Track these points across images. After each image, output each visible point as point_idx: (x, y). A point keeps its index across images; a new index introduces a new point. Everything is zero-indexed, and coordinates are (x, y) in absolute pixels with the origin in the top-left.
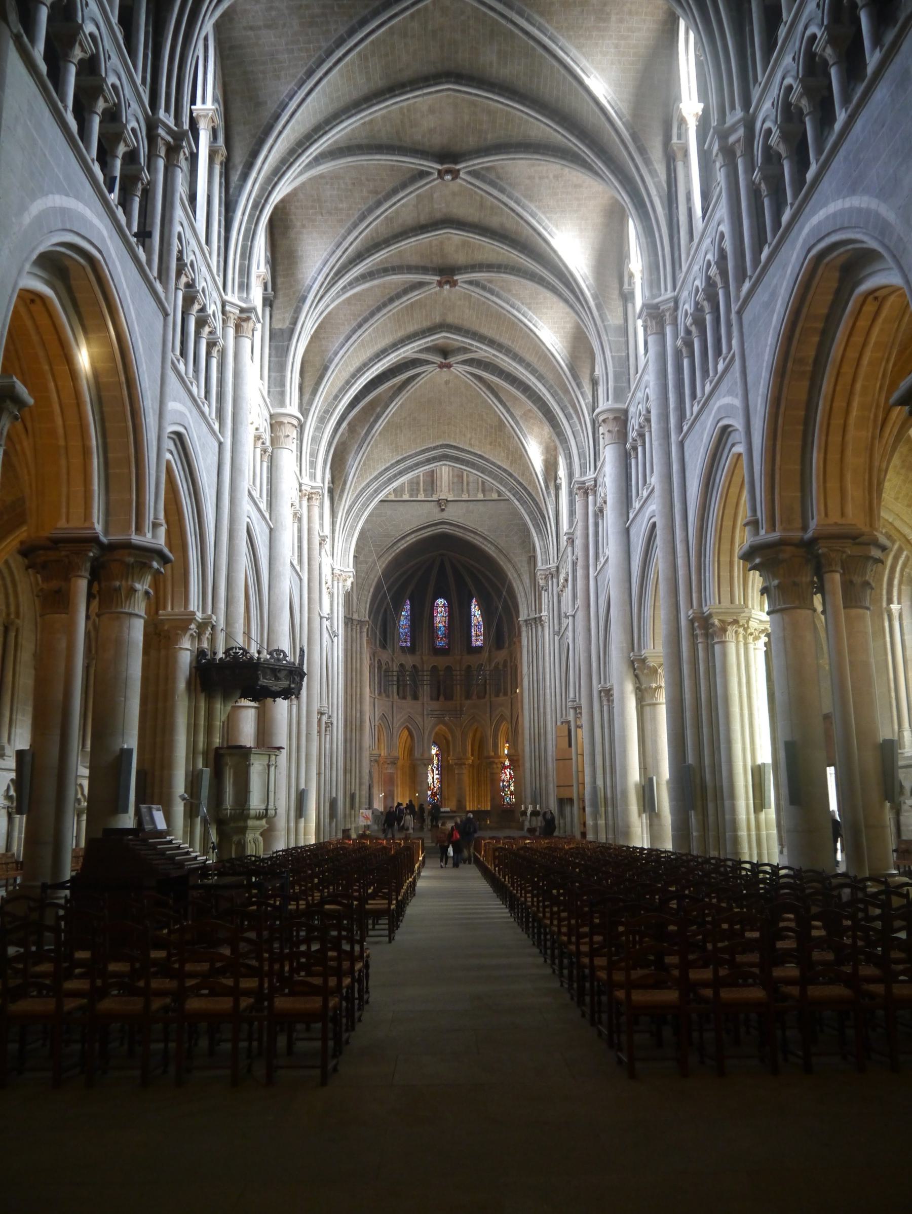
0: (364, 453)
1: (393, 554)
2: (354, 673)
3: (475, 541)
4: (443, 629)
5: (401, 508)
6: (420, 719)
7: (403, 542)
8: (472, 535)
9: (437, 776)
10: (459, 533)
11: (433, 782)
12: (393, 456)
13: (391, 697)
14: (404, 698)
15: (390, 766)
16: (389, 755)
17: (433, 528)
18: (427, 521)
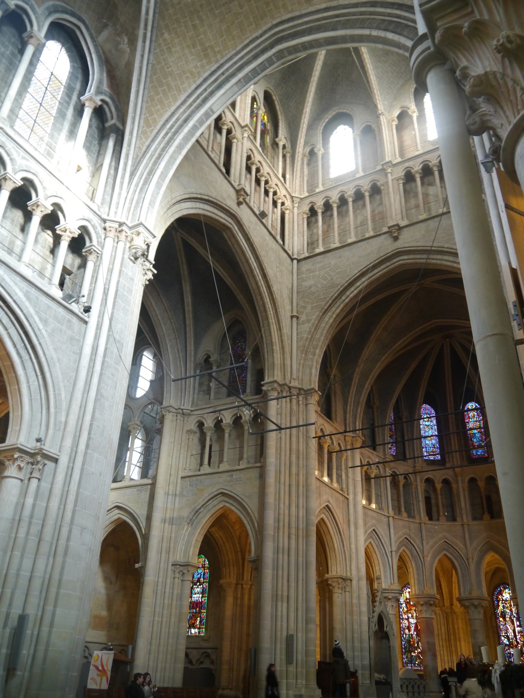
0: (142, 56)
1: (342, 305)
2: (294, 456)
3: (444, 263)
4: (478, 435)
5: (346, 253)
6: (462, 546)
7: (352, 289)
8: (439, 257)
9: (519, 629)
10: (421, 259)
11: (515, 636)
12: (203, 66)
13: (417, 517)
14: (438, 520)
15: (424, 608)
16: (423, 592)
17: (388, 264)
18: (378, 257)
